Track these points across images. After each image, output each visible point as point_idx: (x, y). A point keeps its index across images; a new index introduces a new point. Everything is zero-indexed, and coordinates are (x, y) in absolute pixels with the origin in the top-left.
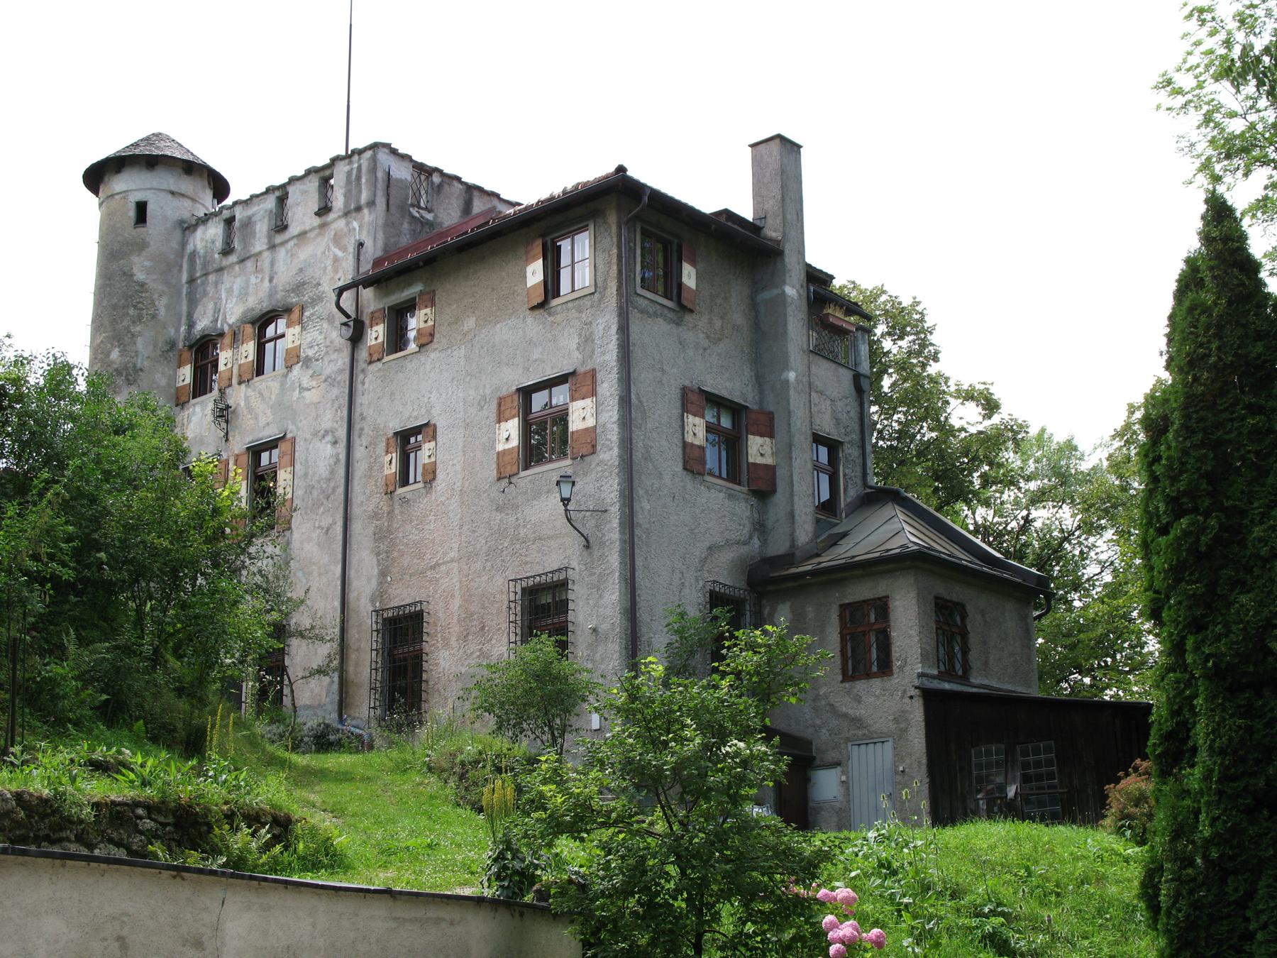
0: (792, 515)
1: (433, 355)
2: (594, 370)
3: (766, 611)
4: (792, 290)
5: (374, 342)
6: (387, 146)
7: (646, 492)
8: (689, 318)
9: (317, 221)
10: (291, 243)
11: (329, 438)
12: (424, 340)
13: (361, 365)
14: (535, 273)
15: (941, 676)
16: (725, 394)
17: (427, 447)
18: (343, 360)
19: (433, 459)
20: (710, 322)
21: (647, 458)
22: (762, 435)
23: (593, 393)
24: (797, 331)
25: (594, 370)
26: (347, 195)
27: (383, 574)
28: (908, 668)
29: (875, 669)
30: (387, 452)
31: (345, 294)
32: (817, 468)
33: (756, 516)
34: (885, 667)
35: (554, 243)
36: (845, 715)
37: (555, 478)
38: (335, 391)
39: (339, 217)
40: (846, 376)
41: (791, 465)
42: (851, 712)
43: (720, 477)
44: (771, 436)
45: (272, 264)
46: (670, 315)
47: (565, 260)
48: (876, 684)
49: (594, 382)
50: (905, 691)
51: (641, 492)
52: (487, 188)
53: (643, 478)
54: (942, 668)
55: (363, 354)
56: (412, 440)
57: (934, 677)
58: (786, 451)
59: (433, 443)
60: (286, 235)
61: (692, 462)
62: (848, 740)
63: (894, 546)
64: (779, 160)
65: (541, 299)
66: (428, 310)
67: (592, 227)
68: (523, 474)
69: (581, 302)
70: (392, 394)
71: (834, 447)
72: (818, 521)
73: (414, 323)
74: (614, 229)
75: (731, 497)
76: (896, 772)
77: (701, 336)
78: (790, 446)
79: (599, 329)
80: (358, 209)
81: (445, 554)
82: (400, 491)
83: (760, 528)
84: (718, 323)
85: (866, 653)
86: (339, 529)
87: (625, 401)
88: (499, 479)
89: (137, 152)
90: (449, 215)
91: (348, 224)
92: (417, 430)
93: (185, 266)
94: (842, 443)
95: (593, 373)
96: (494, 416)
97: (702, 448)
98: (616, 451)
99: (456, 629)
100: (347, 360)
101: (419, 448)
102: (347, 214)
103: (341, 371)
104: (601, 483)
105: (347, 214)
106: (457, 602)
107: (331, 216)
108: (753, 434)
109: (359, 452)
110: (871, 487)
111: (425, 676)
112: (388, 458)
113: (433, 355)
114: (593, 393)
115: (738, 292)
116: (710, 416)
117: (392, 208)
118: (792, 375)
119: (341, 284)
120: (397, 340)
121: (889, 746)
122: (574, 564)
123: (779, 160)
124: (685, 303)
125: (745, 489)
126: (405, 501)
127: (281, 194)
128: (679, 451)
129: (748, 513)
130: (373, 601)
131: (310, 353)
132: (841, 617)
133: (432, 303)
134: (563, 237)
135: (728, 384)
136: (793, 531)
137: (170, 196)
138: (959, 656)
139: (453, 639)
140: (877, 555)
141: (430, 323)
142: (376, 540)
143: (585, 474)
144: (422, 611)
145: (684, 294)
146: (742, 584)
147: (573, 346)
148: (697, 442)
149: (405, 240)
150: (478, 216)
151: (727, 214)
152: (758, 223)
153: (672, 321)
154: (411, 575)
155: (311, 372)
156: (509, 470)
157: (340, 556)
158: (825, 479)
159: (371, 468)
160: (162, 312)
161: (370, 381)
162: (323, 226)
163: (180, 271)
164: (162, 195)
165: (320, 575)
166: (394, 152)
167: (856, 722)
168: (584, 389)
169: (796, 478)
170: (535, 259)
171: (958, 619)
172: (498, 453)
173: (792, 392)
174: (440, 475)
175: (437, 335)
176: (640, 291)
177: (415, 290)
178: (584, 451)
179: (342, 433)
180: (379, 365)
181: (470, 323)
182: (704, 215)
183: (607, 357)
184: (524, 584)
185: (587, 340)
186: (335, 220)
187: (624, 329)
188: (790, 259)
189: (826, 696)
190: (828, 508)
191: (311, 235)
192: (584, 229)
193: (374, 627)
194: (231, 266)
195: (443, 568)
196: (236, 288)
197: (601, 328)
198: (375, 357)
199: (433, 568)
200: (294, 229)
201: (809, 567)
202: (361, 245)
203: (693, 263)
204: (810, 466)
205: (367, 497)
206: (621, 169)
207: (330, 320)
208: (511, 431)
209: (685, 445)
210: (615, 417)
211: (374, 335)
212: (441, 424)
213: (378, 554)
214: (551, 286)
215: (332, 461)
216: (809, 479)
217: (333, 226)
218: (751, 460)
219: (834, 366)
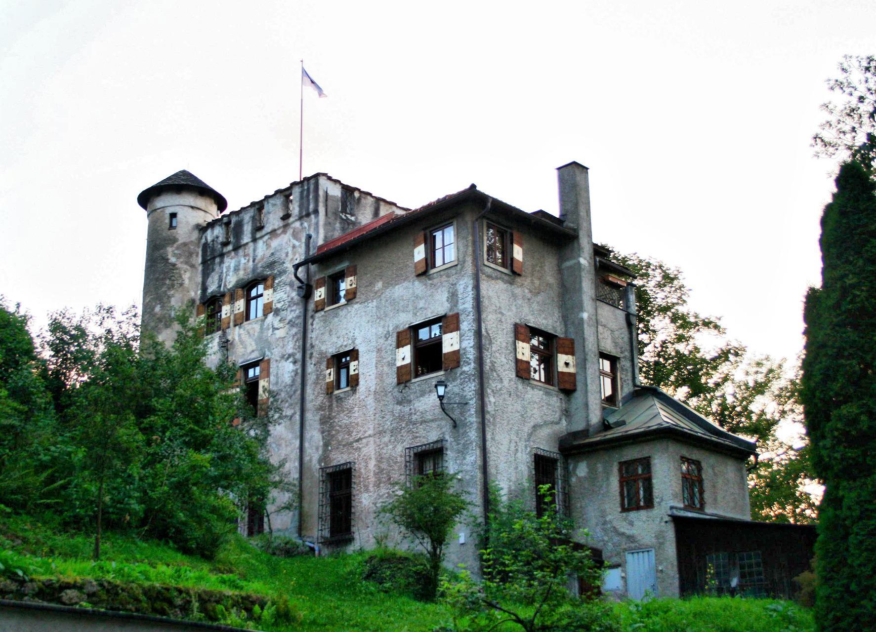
0: (586, 405)
1: (356, 306)
2: (458, 314)
3: (571, 467)
4: (585, 260)
5: (318, 299)
6: (325, 175)
7: (493, 391)
8: (518, 280)
9: (281, 223)
10: (266, 237)
11: (291, 360)
12: (350, 297)
13: (310, 313)
14: (420, 253)
16: (543, 328)
18: (297, 311)
19: (356, 372)
20: (532, 282)
21: (493, 369)
22: (567, 354)
23: (457, 328)
24: (588, 286)
25: (458, 314)
26: (301, 206)
27: (326, 445)
28: (663, 504)
29: (642, 504)
30: (328, 368)
31: (300, 269)
33: (564, 405)
34: (649, 503)
35: (431, 234)
36: (623, 534)
37: (434, 383)
38: (294, 330)
39: (296, 220)
40: (621, 315)
41: (585, 373)
42: (626, 531)
44: (573, 354)
45: (254, 250)
46: (506, 278)
47: (439, 244)
48: (643, 514)
50: (662, 518)
51: (489, 391)
53: (491, 382)
54: (686, 503)
55: (311, 306)
56: (344, 360)
57: (680, 509)
58: (582, 364)
59: (356, 362)
60: (264, 232)
61: (522, 371)
62: (625, 550)
63: (654, 425)
65: (423, 270)
66: (352, 278)
67: (455, 223)
69: (449, 271)
70: (331, 331)
71: (613, 360)
72: (604, 409)
73: (345, 286)
74: (470, 225)
75: (547, 393)
76: (657, 571)
77: (527, 291)
78: (585, 360)
79: (460, 288)
80: (308, 215)
81: (365, 432)
83: (567, 413)
84: (537, 282)
85: (637, 493)
87: (478, 334)
89: (170, 182)
90: (365, 217)
91: (302, 224)
94: (619, 358)
95: (457, 316)
96: (394, 344)
98: (473, 365)
99: (372, 479)
100: (302, 310)
102: (301, 218)
103: (298, 317)
105: (301, 218)
106: (372, 464)
107: (291, 219)
109: (310, 368)
110: (638, 386)
111: (353, 510)
112: (328, 371)
114: (457, 328)
115: (549, 263)
117: (330, 214)
118: (585, 315)
119: (297, 262)
120: (333, 297)
121: (653, 553)
122: (447, 437)
124: (515, 269)
125: (556, 389)
126: (339, 399)
127: (258, 206)
128: (513, 364)
129: (558, 404)
131: (279, 306)
132: (620, 470)
133: (354, 273)
134: (437, 230)
135: (544, 321)
136: (587, 417)
137: (190, 209)
138: (697, 495)
139: (371, 486)
140: (642, 430)
141: (354, 286)
143: (454, 380)
144: (350, 469)
145: (515, 265)
146: (556, 450)
147: (445, 299)
148: (525, 359)
149: (337, 234)
150: (383, 217)
151: (541, 213)
152: (562, 218)
153: (506, 282)
154: (344, 446)
155: (279, 318)
156: (405, 378)
157: (298, 434)
158: (608, 382)
159: (318, 378)
160: (187, 282)
162: (286, 226)
163: (197, 256)
164: (186, 209)
165: (287, 446)
166: (330, 178)
167: (631, 538)
169: (589, 381)
172: (398, 368)
173: (585, 326)
174: (362, 381)
175: (358, 294)
176: (486, 263)
179: (299, 356)
180: (322, 313)
181: (379, 285)
182: (526, 213)
183: (465, 306)
184: (415, 451)
185: (453, 297)
186: (293, 222)
187: (477, 287)
188: (583, 241)
189: (610, 522)
191: (279, 232)
192: (450, 224)
193: (321, 479)
194: (229, 252)
195: (364, 441)
196: (232, 265)
197: (462, 287)
198: (320, 308)
199: (357, 441)
200: (268, 228)
201: (598, 439)
203: (521, 245)
204: (597, 373)
205: (314, 396)
207: (291, 285)
209: (517, 361)
210: (472, 344)
211: (319, 294)
212: (362, 350)
213: (323, 432)
215: (293, 374)
216: (597, 382)
217: (293, 225)
218: (560, 370)
219: (612, 308)
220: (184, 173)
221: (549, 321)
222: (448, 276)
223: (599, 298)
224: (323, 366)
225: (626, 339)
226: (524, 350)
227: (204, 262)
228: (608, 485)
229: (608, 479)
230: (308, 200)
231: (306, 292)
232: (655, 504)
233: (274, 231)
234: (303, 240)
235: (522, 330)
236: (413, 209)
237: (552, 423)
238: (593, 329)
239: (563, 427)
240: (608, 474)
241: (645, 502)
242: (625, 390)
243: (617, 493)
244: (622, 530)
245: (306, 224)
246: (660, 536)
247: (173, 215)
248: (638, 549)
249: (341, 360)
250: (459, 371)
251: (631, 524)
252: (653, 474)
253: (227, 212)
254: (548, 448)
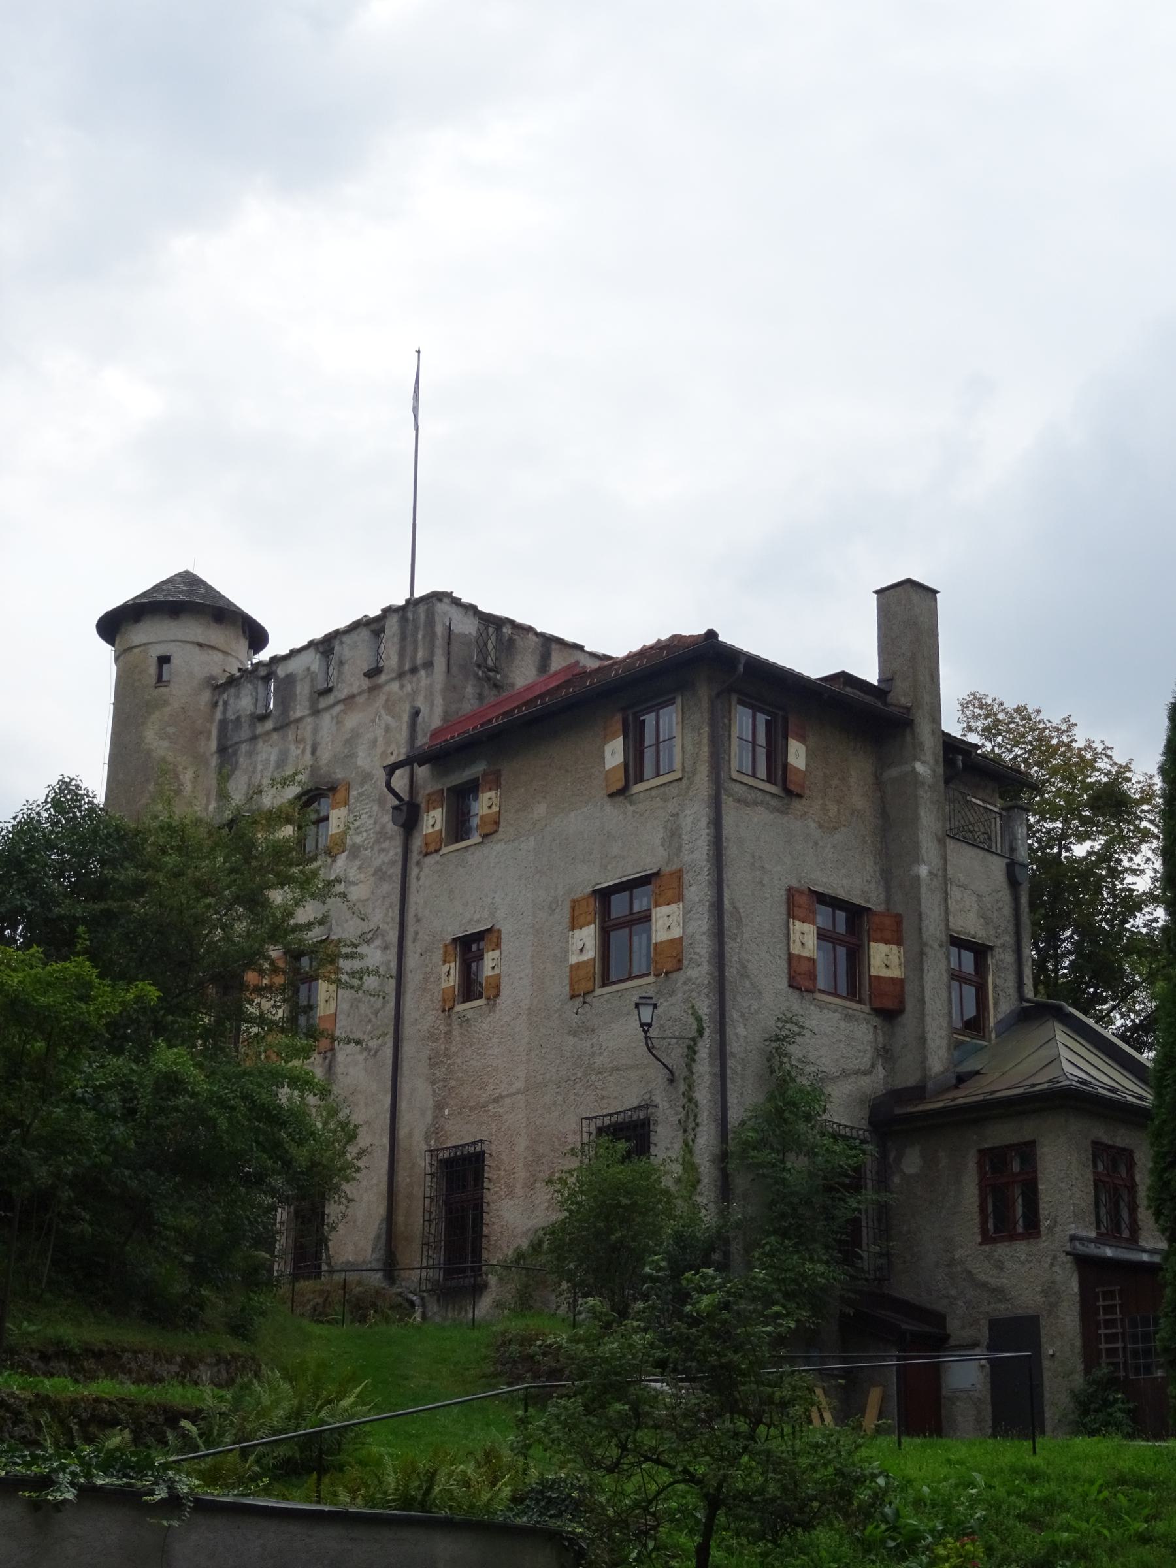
0: (922, 1040)
1: (499, 847)
2: (681, 870)
4: (925, 768)
5: (430, 830)
6: (448, 595)
7: (743, 1015)
8: (797, 805)
9: (366, 683)
10: (338, 708)
11: (378, 942)
12: (487, 830)
13: (415, 856)
14: (614, 753)
16: (842, 894)
17: (490, 957)
18: (394, 849)
19: (497, 971)
20: (824, 808)
21: (744, 975)
22: (887, 942)
23: (680, 898)
24: (928, 821)
25: (681, 870)
26: (402, 654)
27: (439, 1107)
28: (1058, 1229)
29: (1020, 1230)
30: (445, 962)
31: (398, 772)
32: (956, 976)
33: (881, 1039)
34: (1032, 1228)
35: (636, 716)
36: (984, 1285)
37: (636, 999)
38: (386, 887)
39: (393, 679)
40: (998, 866)
41: (921, 978)
42: (992, 1281)
43: (835, 995)
44: (899, 943)
45: (315, 731)
46: (773, 802)
47: (649, 739)
48: (1021, 1249)
49: (680, 885)
50: (1055, 1258)
51: (736, 1015)
52: (569, 638)
53: (739, 998)
54: (1103, 1230)
55: (417, 843)
56: (474, 947)
57: (1090, 1240)
58: (916, 962)
60: (331, 699)
61: (800, 978)
63: (1042, 1080)
64: (907, 612)
65: (621, 784)
67: (679, 701)
68: (598, 992)
69: (667, 789)
70: (451, 892)
71: (981, 951)
72: (958, 1045)
73: (484, 805)
74: (705, 703)
75: (848, 1017)
77: (813, 825)
78: (922, 954)
79: (687, 822)
80: (414, 670)
81: (511, 1084)
82: (460, 1008)
83: (886, 1054)
84: (833, 809)
85: (1010, 1208)
86: (388, 1051)
87: (718, 908)
88: (572, 997)
89: (159, 598)
90: (523, 675)
92: (480, 936)
93: (214, 733)
94: (991, 948)
95: (679, 874)
96: (566, 920)
97: (812, 960)
98: (705, 967)
99: (521, 1174)
100: (400, 850)
101: (481, 957)
102: (401, 675)
103: (392, 863)
105: (401, 675)
106: (522, 1144)
107: (383, 678)
108: (877, 941)
109: (412, 961)
110: (1028, 1001)
111: (486, 1231)
112: (446, 968)
113: (496, 848)
114: (680, 898)
115: (858, 771)
116: (823, 916)
117: (454, 670)
118: (923, 871)
119: (391, 760)
120: (459, 827)
122: (657, 1099)
123: (907, 612)
124: (791, 787)
125: (866, 1008)
126: (464, 1020)
127: (326, 646)
128: (784, 965)
129: (871, 1037)
130: (427, 1139)
131: (358, 840)
132: (980, 1166)
133: (497, 785)
134: (648, 711)
135: (845, 882)
136: (924, 1059)
137: (197, 648)
138: (1125, 1214)
139: (519, 1186)
140: (1021, 1090)
141: (495, 809)
142: (431, 1066)
143: (672, 993)
144: (483, 1153)
145: (791, 777)
146: (864, 1124)
147: (658, 841)
148: (806, 954)
149: (469, 706)
150: (556, 673)
151: (844, 678)
152: (883, 686)
153: (775, 810)
154: (471, 1109)
155: (358, 863)
156: (583, 986)
157: (389, 1083)
158: (970, 992)
159: (426, 980)
160: (188, 787)
161: (425, 876)
162: (373, 689)
163: (208, 738)
164: (188, 647)
165: (366, 1105)
166: (457, 602)
169: (928, 994)
170: (615, 737)
171: (1123, 1171)
172: (572, 966)
173: (923, 890)
174: (505, 990)
175: (502, 824)
176: (735, 775)
177: (478, 769)
178: (669, 966)
179: (393, 936)
180: (437, 857)
183: (695, 856)
184: (599, 1123)
185: (673, 834)
187: (716, 823)
188: (924, 730)
190: (975, 1026)
191: (361, 700)
192: (671, 702)
193: (428, 1170)
194: (268, 733)
195: (508, 1101)
196: (273, 758)
197: (689, 820)
198: (432, 848)
199: (496, 1100)
200: (342, 693)
201: (941, 1105)
202: (417, 713)
203: (802, 739)
204: (945, 978)
205: (421, 1015)
207: (381, 802)
208: (586, 939)
209: (791, 957)
210: (705, 928)
211: (431, 822)
212: (506, 928)
213: (433, 1083)
214: (634, 770)
216: (945, 995)
218: (874, 972)
219: (981, 853)
221: (854, 881)
222: (666, 800)
223: (959, 833)
224: (438, 955)
225: (1007, 911)
226: (805, 938)
227: (222, 750)
230: (415, 642)
231: (408, 816)
233: (352, 697)
234: (406, 718)
235: (802, 900)
236: (619, 650)
237: (857, 1072)
238: (939, 896)
239: (875, 1082)
242: (1001, 1006)
243: (975, 1208)
244: (983, 1277)
246: (1050, 1290)
247: (164, 660)
249: (469, 948)
250: (680, 977)
253: (265, 655)
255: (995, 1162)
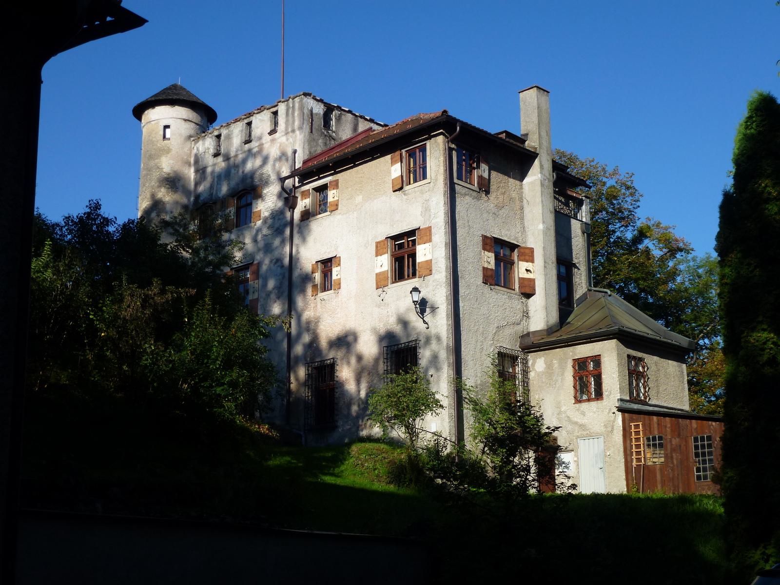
3: (530, 363)
15: (631, 401)
19: (339, 277)
28: (612, 396)
34: (599, 395)
36: (576, 423)
42: (579, 421)
46: (475, 194)
48: (593, 404)
59: (339, 268)
62: (578, 437)
65: (399, 186)
66: (334, 191)
76: (605, 456)
88: (377, 289)
91: (287, 140)
95: (429, 229)
104: (436, 288)
114: (430, 240)
121: (602, 440)
167: (582, 426)
168: (425, 238)
172: (377, 274)
181: (359, 199)
182: (490, 134)
185: (426, 210)
186: (280, 137)
189: (565, 412)
197: (434, 203)
206: (445, 112)
215: (281, 277)
217: (279, 141)
220: (175, 87)
228: (562, 379)
229: (563, 374)
232: (604, 396)
235: (489, 241)
240: (563, 368)
241: (595, 395)
244: (575, 420)
245: (291, 140)
248: (591, 436)
251: (583, 414)
252: (603, 371)
254: (511, 345)
255: (580, 364)
